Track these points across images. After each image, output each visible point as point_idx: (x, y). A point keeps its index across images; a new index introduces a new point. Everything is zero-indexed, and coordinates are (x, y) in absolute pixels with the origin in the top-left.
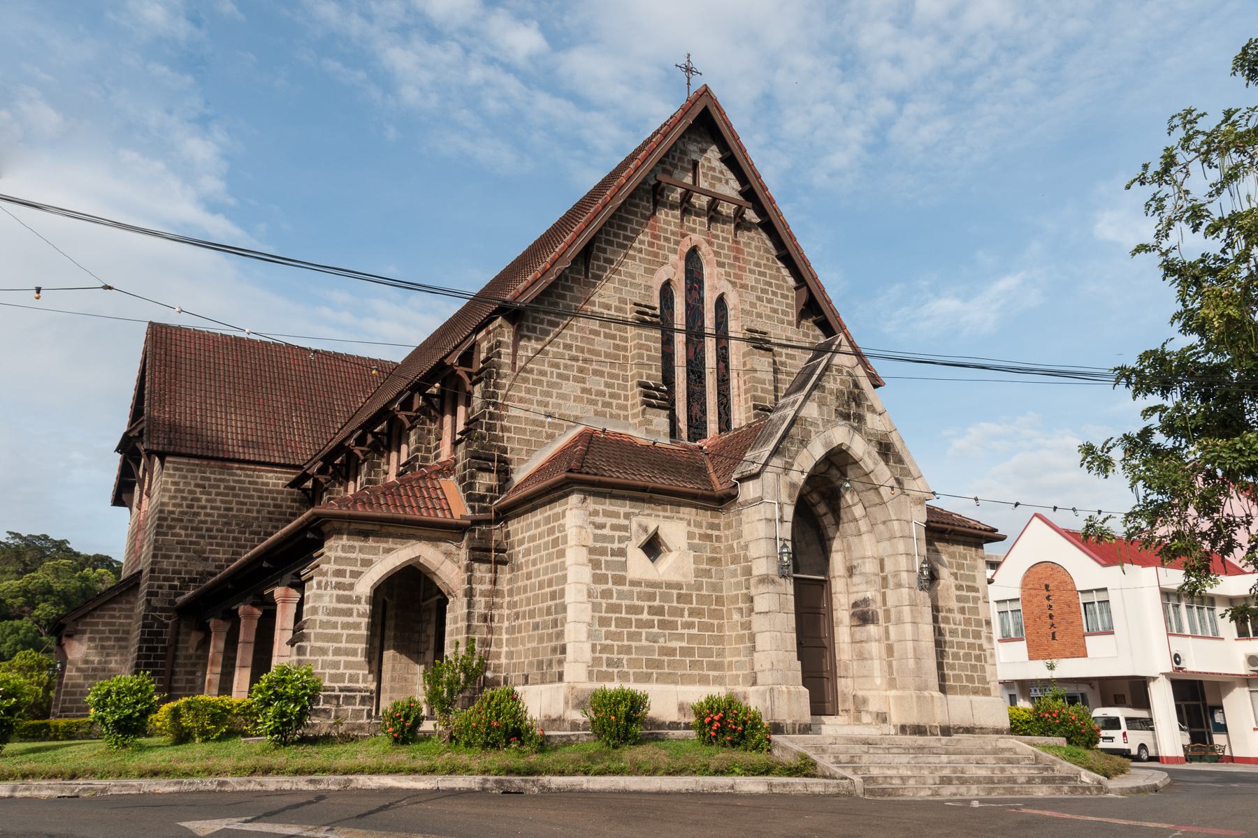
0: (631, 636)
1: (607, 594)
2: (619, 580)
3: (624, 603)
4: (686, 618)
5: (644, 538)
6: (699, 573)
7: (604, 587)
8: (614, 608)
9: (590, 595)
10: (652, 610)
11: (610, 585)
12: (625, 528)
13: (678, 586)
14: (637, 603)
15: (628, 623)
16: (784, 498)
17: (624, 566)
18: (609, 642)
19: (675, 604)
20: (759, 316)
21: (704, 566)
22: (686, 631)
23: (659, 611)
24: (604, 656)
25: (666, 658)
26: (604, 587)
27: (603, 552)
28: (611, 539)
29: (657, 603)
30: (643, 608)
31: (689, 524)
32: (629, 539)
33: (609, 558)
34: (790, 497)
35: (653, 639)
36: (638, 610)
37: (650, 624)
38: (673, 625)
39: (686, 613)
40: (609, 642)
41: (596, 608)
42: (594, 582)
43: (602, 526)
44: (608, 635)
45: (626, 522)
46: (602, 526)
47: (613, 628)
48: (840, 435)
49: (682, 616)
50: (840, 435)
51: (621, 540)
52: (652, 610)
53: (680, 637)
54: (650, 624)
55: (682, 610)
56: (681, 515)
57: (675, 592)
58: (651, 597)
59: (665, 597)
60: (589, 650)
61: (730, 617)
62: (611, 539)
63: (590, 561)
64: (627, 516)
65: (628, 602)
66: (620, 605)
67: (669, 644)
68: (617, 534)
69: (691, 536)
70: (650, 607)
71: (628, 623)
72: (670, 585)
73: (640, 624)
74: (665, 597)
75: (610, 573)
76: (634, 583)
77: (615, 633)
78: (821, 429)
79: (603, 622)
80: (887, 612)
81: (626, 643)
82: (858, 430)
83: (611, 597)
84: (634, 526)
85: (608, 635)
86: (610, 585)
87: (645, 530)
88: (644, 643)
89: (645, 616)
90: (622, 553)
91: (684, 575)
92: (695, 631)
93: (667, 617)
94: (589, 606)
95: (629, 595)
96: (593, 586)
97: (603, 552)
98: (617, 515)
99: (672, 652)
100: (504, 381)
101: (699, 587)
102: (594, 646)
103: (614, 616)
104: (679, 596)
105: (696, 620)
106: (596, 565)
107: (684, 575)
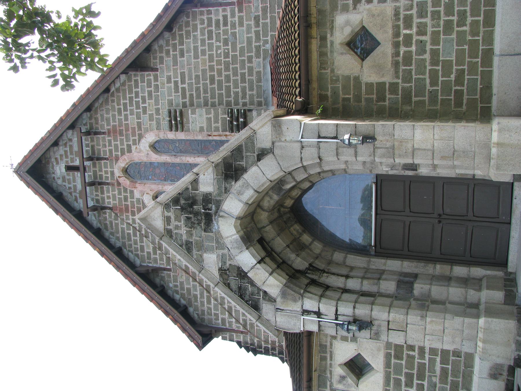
16: (297, 307)
19: (404, 362)
20: (157, 110)
25: (450, 378)
34: (295, 301)
38: (422, 367)
48: (228, 229)
50: (228, 229)
56: (328, 344)
57: (393, 361)
78: (226, 251)
82: (219, 204)
93: (415, 372)
100: (256, 341)
104: (397, 357)
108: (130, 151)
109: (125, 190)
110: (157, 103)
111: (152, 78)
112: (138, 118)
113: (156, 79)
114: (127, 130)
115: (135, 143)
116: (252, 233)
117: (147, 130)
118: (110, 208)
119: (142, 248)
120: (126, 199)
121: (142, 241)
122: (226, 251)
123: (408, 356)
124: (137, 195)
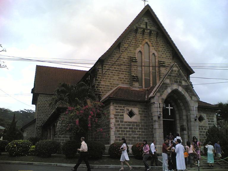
0: (125, 134)
1: (119, 125)
2: (122, 122)
3: (123, 127)
4: (138, 130)
5: (128, 112)
6: (141, 120)
7: (118, 123)
8: (121, 128)
9: (115, 125)
10: (130, 128)
11: (120, 123)
12: (123, 110)
13: (136, 123)
14: (126, 127)
15: (124, 131)
17: (123, 118)
18: (119, 135)
21: (143, 118)
22: (138, 133)
23: (131, 128)
24: (118, 139)
26: (118, 123)
27: (118, 115)
28: (120, 112)
29: (131, 127)
30: (128, 128)
31: (139, 108)
32: (124, 112)
33: (119, 117)
35: (130, 135)
36: (127, 128)
37: (129, 131)
38: (135, 132)
39: (138, 129)
40: (119, 135)
41: (116, 128)
42: (116, 122)
43: (118, 110)
44: (119, 134)
45: (124, 108)
46: (118, 110)
47: (120, 132)
49: (137, 129)
51: (122, 112)
52: (130, 128)
53: (137, 134)
54: (129, 131)
55: (137, 128)
56: (137, 107)
57: (135, 124)
58: (129, 125)
59: (133, 125)
60: (115, 138)
61: (149, 130)
62: (120, 112)
63: (115, 117)
64: (124, 107)
65: (124, 126)
66: (122, 127)
67: (134, 136)
68: (121, 111)
69: (139, 111)
70: (129, 127)
71: (124, 131)
72: (134, 122)
73: (127, 131)
74: (133, 125)
75: (120, 120)
76: (125, 122)
77: (121, 134)
79: (118, 131)
80: (188, 128)
81: (123, 136)
83: (120, 125)
84: (125, 109)
85: (119, 134)
86: (120, 123)
87: (128, 110)
88: (128, 136)
89: (128, 130)
90: (122, 115)
91: (138, 120)
92: (140, 133)
93: (133, 130)
94: (115, 128)
95: (124, 125)
96: (115, 123)
97: (118, 115)
98: (121, 107)
99: (135, 138)
101: (141, 123)
102: (116, 137)
103: (121, 130)
105: (141, 130)
106: (116, 118)
107: (138, 120)
108: (153, 46)
109: (142, 42)
110: (165, 58)
111: (171, 58)
112: (161, 51)
113: (171, 59)
114: (158, 47)
115: (155, 48)
116: (175, 92)
117: (158, 53)
118: (136, 35)
119: (125, 43)
120: (139, 41)
121: (127, 43)
122: (170, 85)
123: (137, 128)
124: (141, 45)
